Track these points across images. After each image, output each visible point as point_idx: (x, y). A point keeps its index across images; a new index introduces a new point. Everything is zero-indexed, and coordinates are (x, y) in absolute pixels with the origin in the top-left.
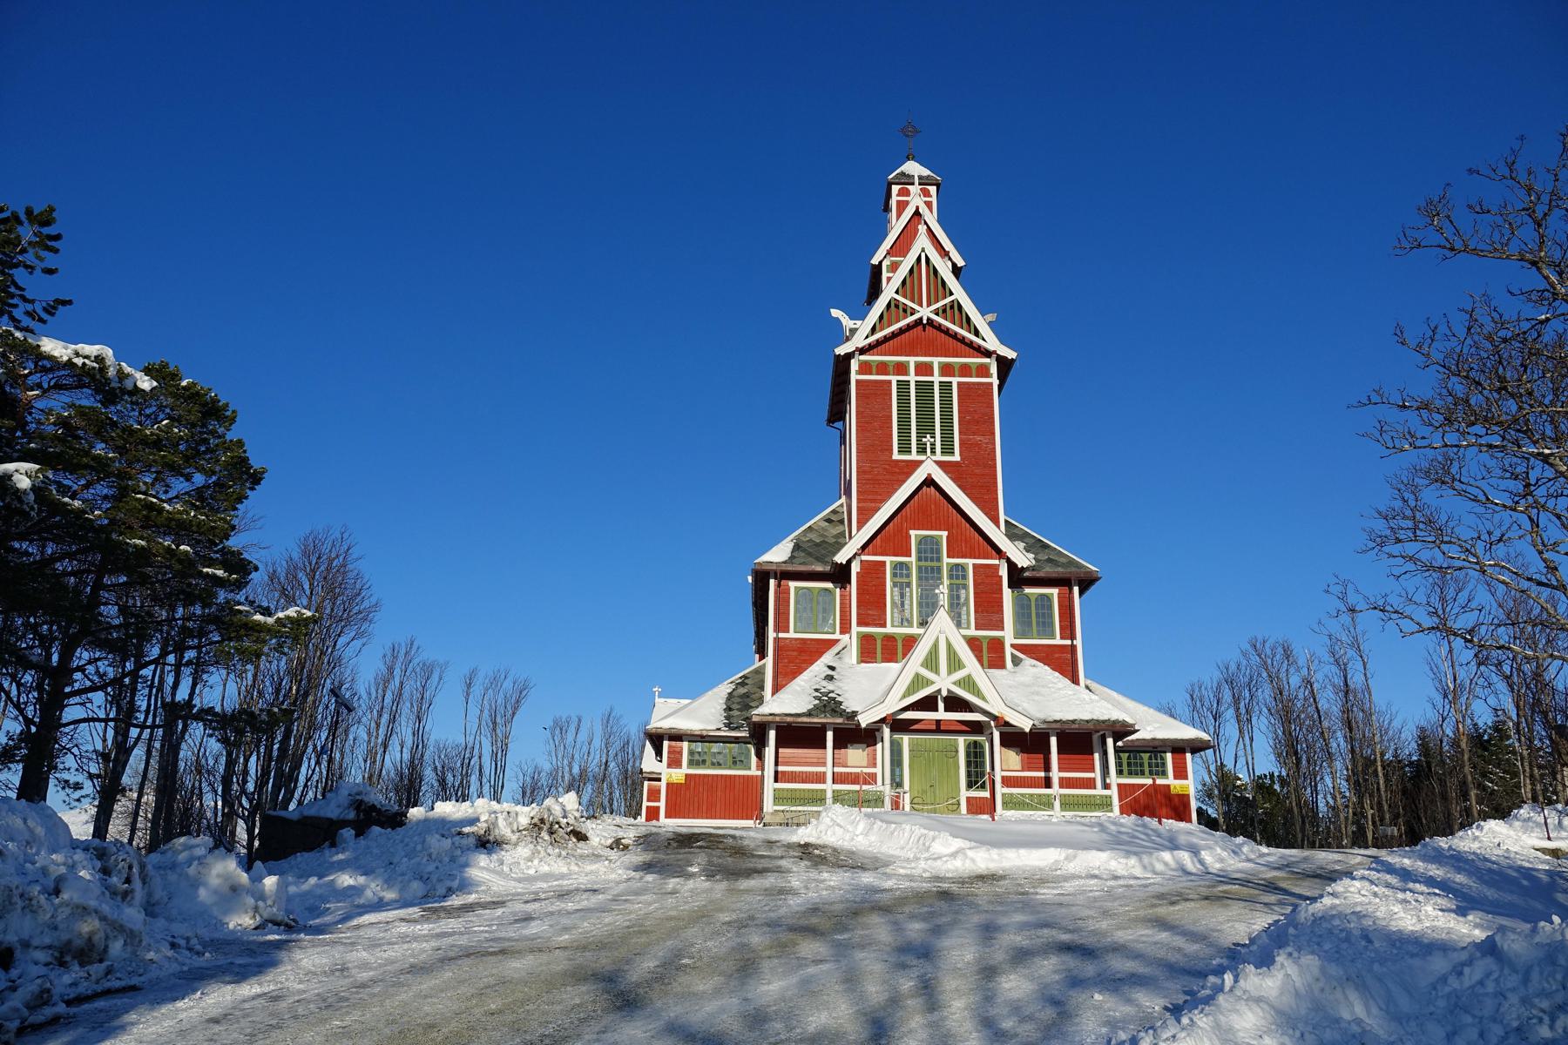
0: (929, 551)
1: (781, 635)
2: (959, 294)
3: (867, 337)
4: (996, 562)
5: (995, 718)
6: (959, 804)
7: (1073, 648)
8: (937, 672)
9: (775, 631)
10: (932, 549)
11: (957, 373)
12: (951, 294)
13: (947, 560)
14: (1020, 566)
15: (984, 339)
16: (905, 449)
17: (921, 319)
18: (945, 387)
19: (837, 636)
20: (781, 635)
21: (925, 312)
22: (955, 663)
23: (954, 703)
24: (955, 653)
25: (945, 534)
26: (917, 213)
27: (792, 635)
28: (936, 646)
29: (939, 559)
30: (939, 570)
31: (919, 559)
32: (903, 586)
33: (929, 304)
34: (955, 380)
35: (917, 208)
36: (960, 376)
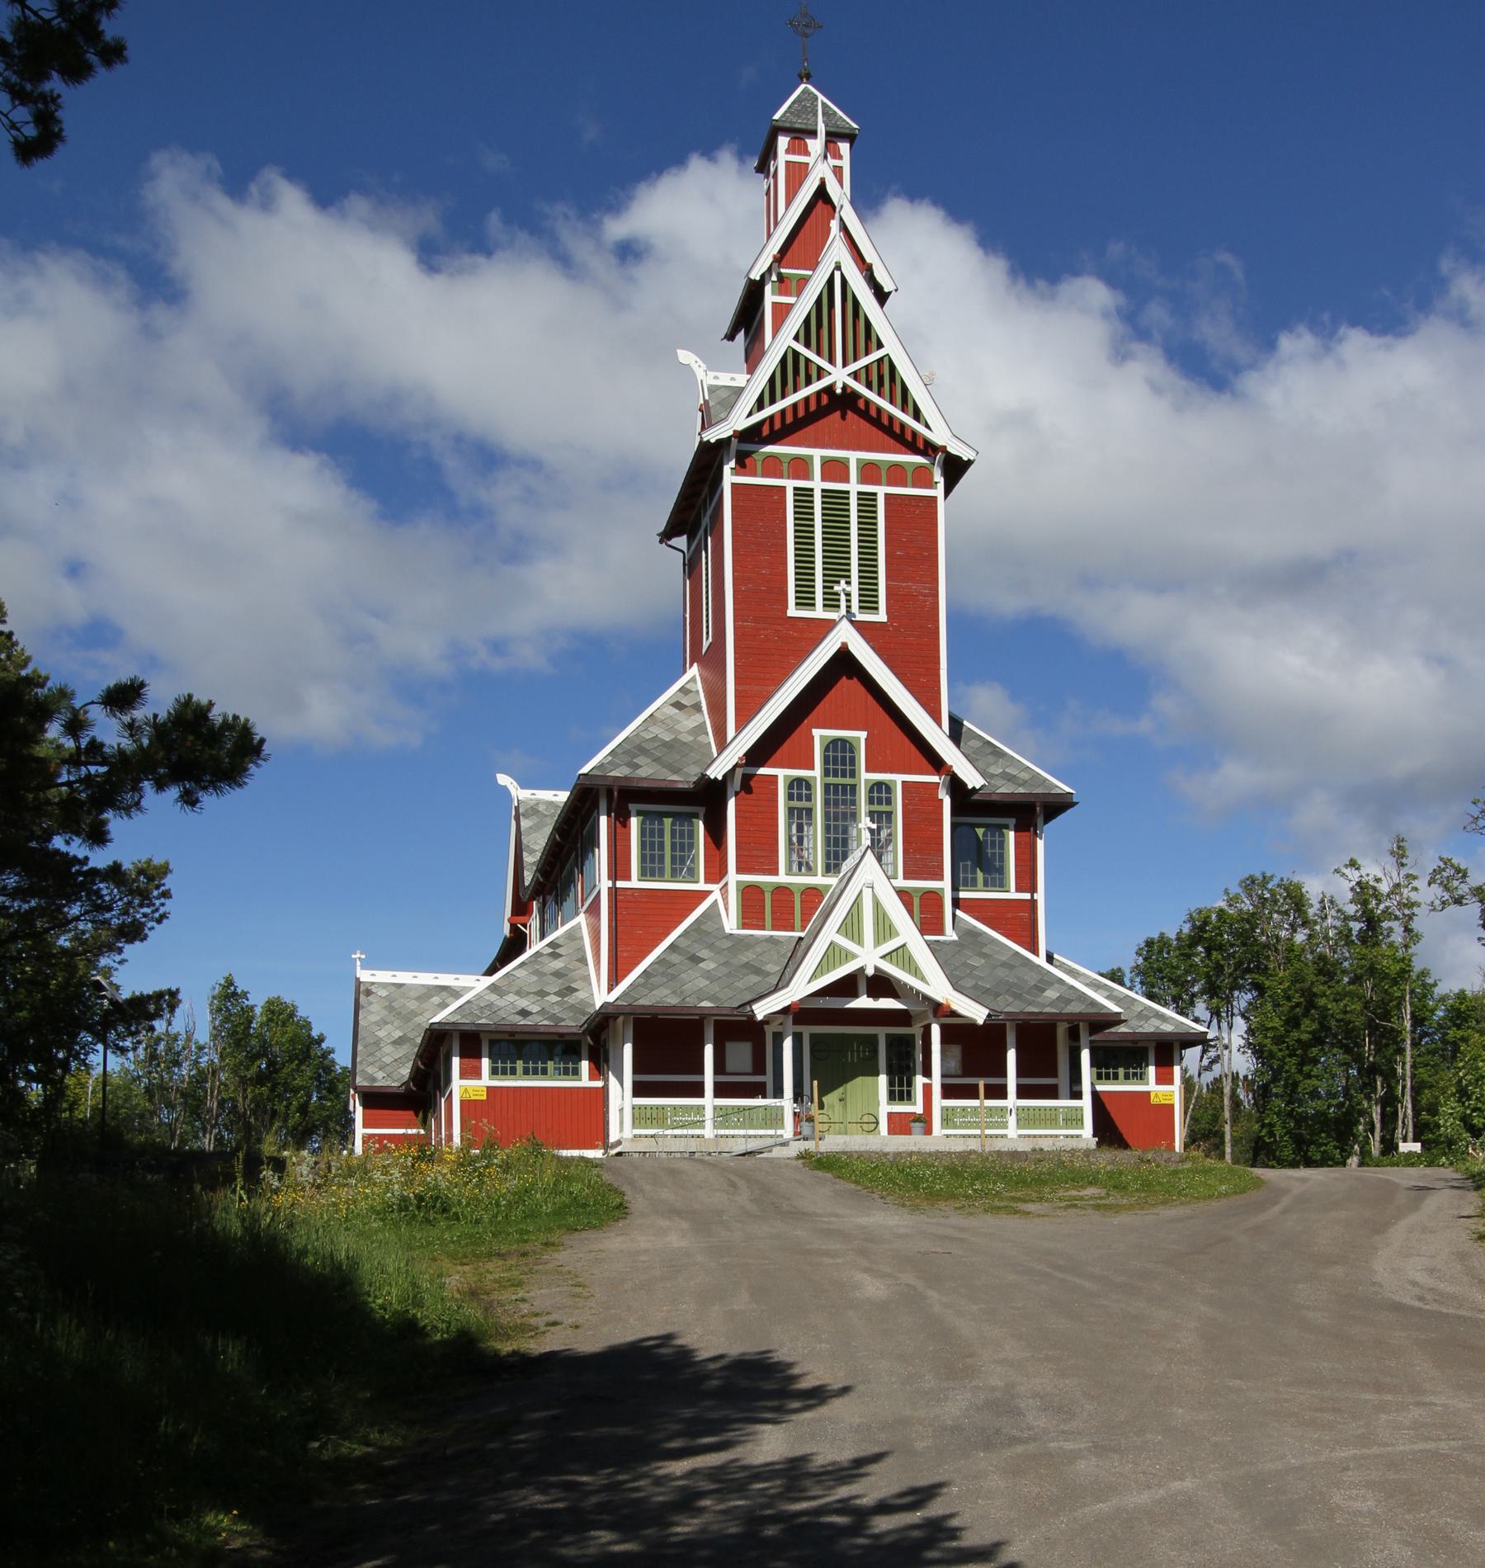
0: (839, 756)
3: (750, 414)
4: (935, 779)
7: (1033, 903)
8: (860, 942)
10: (844, 758)
11: (884, 479)
13: (865, 777)
15: (927, 426)
16: (805, 600)
18: (867, 500)
22: (884, 929)
23: (881, 985)
25: (863, 735)
28: (858, 902)
29: (853, 774)
30: (854, 788)
31: (826, 773)
34: (881, 491)
36: (889, 484)
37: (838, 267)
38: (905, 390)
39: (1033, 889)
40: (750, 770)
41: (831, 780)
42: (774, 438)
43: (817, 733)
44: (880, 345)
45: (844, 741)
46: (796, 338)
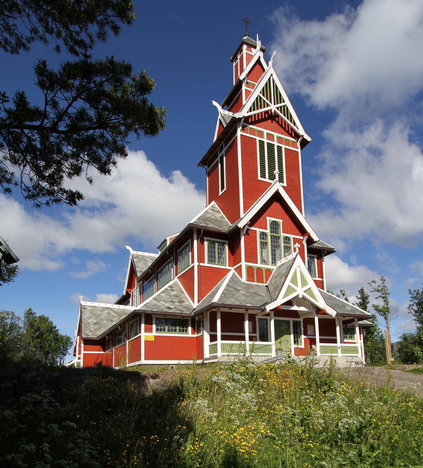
1: (201, 264)
2: (288, 103)
4: (302, 238)
5: (319, 311)
6: (291, 351)
9: (198, 261)
10: (276, 228)
13: (283, 235)
14: (315, 241)
15: (297, 128)
18: (279, 148)
19: (227, 267)
20: (201, 264)
24: (303, 277)
25: (281, 221)
26: (258, 62)
27: (206, 264)
30: (279, 237)
32: (264, 245)
35: (260, 57)
37: (272, 75)
38: (291, 116)
39: (322, 277)
40: (249, 228)
42: (253, 123)
43: (268, 218)
44: (284, 102)
45: (276, 222)
46: (260, 93)
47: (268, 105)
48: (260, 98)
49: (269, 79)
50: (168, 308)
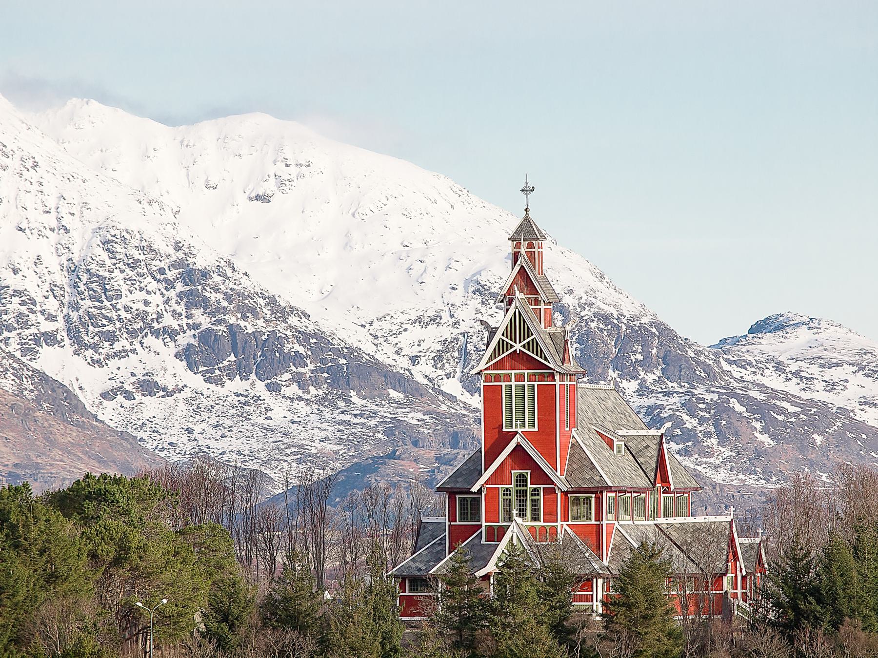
1: (452, 523)
3: (487, 363)
10: (523, 480)
12: (532, 335)
15: (549, 362)
17: (516, 350)
20: (452, 523)
21: (518, 347)
25: (529, 472)
27: (458, 523)
29: (526, 486)
33: (520, 342)
41: (518, 488)
47: (512, 346)
48: (503, 341)
49: (515, 313)
50: (420, 570)
